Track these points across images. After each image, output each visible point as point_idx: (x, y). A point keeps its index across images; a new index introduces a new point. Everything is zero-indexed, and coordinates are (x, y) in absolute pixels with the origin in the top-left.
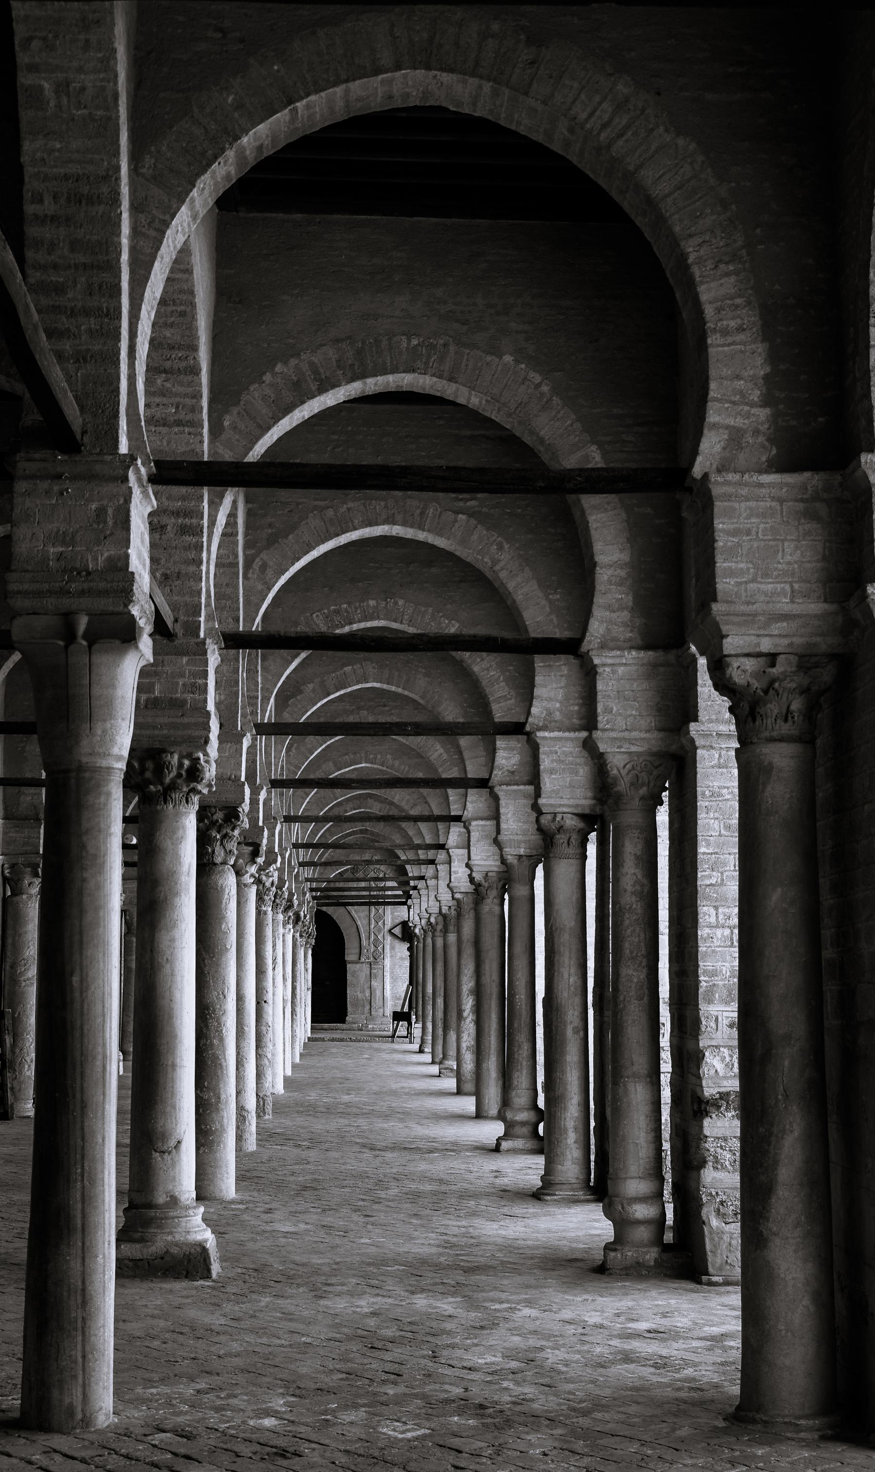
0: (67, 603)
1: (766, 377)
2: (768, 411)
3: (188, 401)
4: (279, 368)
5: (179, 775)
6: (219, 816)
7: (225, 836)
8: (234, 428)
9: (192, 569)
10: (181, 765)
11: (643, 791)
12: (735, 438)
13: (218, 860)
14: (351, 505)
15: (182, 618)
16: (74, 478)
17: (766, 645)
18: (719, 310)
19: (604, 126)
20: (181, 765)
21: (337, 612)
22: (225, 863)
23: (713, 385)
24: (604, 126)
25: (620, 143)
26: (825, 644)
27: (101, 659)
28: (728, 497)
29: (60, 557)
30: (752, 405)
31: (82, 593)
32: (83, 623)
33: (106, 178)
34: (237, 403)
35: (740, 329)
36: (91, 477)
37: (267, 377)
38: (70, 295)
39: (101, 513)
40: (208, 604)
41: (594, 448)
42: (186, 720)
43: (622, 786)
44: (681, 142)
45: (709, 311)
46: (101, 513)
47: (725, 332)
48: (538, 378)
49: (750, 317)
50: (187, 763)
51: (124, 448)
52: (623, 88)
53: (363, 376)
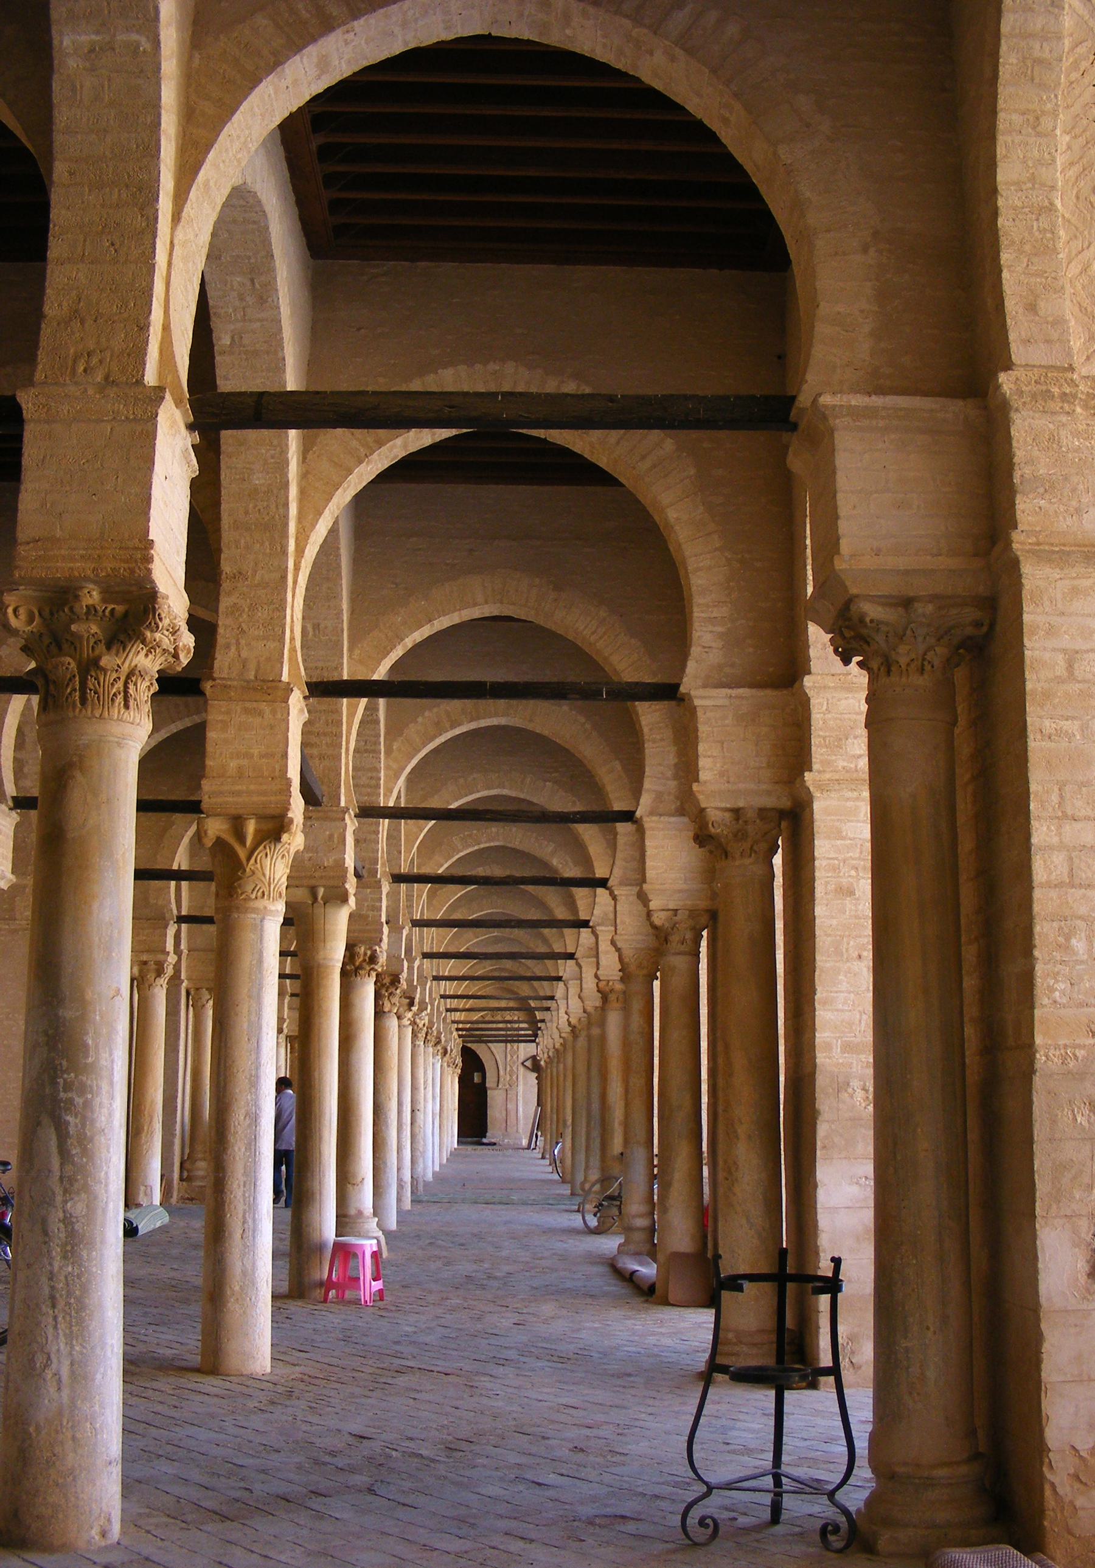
0: (313, 882)
1: (676, 765)
2: (675, 783)
3: (373, 739)
4: (427, 714)
5: (364, 960)
6: (387, 981)
7: (391, 994)
8: (399, 750)
9: (374, 836)
10: (365, 954)
11: (645, 972)
12: (659, 797)
13: (386, 1010)
14: (475, 775)
15: (367, 866)
16: (318, 819)
17: (672, 905)
18: (651, 730)
19: (593, 633)
20: (365, 954)
21: (470, 836)
22: (390, 1012)
23: (647, 769)
24: (593, 633)
25: (601, 641)
26: (703, 904)
27: (330, 910)
28: (653, 829)
29: (310, 859)
30: (668, 779)
31: (321, 877)
32: (321, 891)
33: (336, 668)
34: (401, 735)
35: (662, 740)
36: (326, 818)
37: (420, 719)
38: (317, 725)
39: (331, 836)
40: (382, 857)
41: (617, 762)
42: (368, 928)
43: (632, 968)
44: (633, 641)
45: (646, 730)
46: (331, 836)
47: (654, 741)
48: (583, 720)
49: (668, 733)
50: (369, 953)
51: (343, 804)
52: (603, 613)
53: (478, 718)
